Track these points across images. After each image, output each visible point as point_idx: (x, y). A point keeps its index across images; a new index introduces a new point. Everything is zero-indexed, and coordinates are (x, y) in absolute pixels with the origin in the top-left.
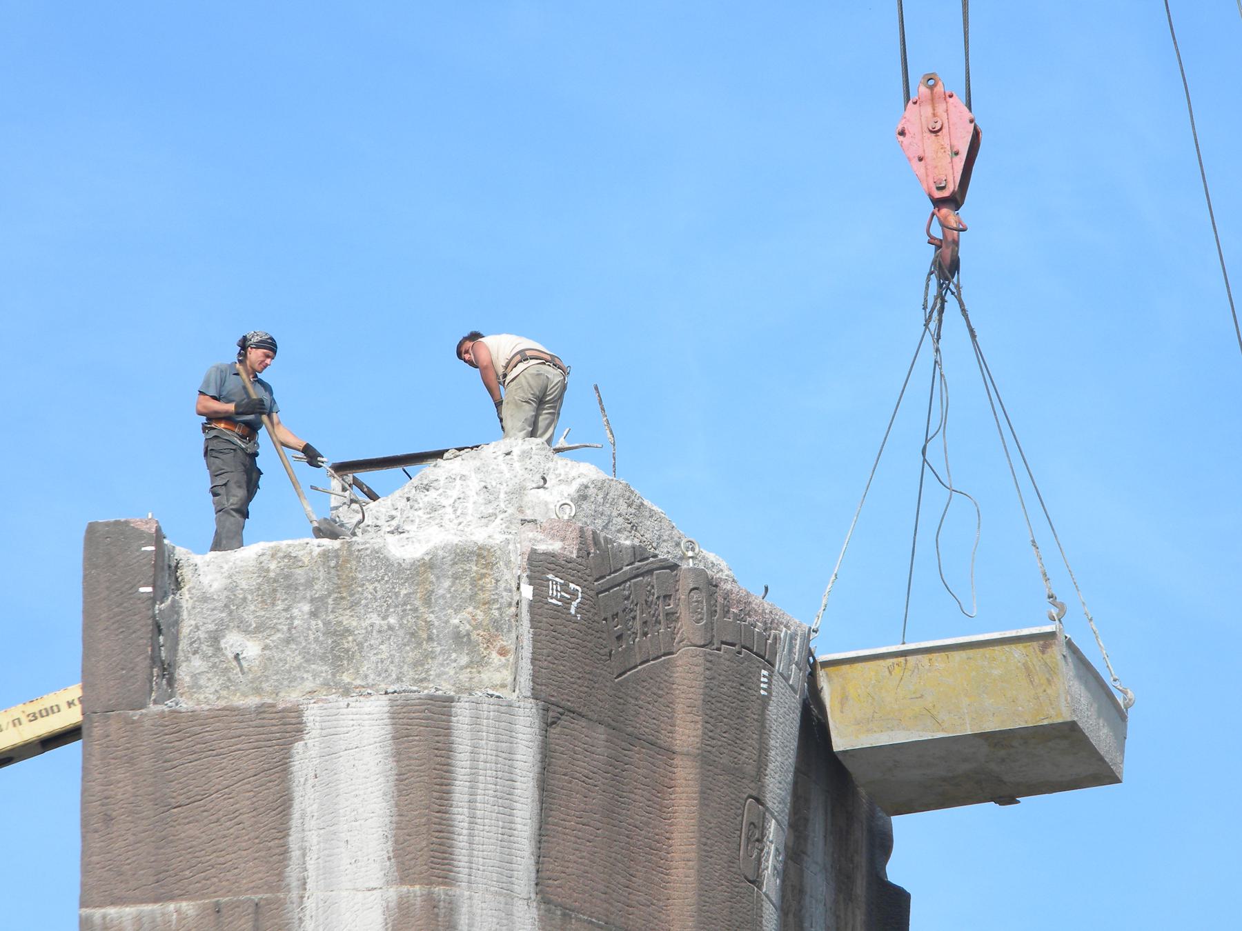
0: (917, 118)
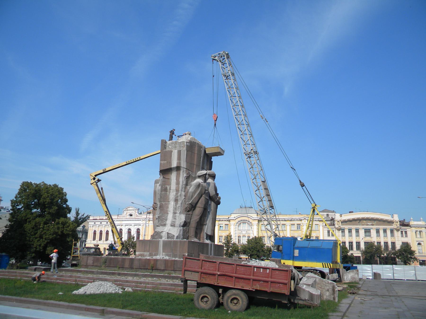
0: (214, 116)
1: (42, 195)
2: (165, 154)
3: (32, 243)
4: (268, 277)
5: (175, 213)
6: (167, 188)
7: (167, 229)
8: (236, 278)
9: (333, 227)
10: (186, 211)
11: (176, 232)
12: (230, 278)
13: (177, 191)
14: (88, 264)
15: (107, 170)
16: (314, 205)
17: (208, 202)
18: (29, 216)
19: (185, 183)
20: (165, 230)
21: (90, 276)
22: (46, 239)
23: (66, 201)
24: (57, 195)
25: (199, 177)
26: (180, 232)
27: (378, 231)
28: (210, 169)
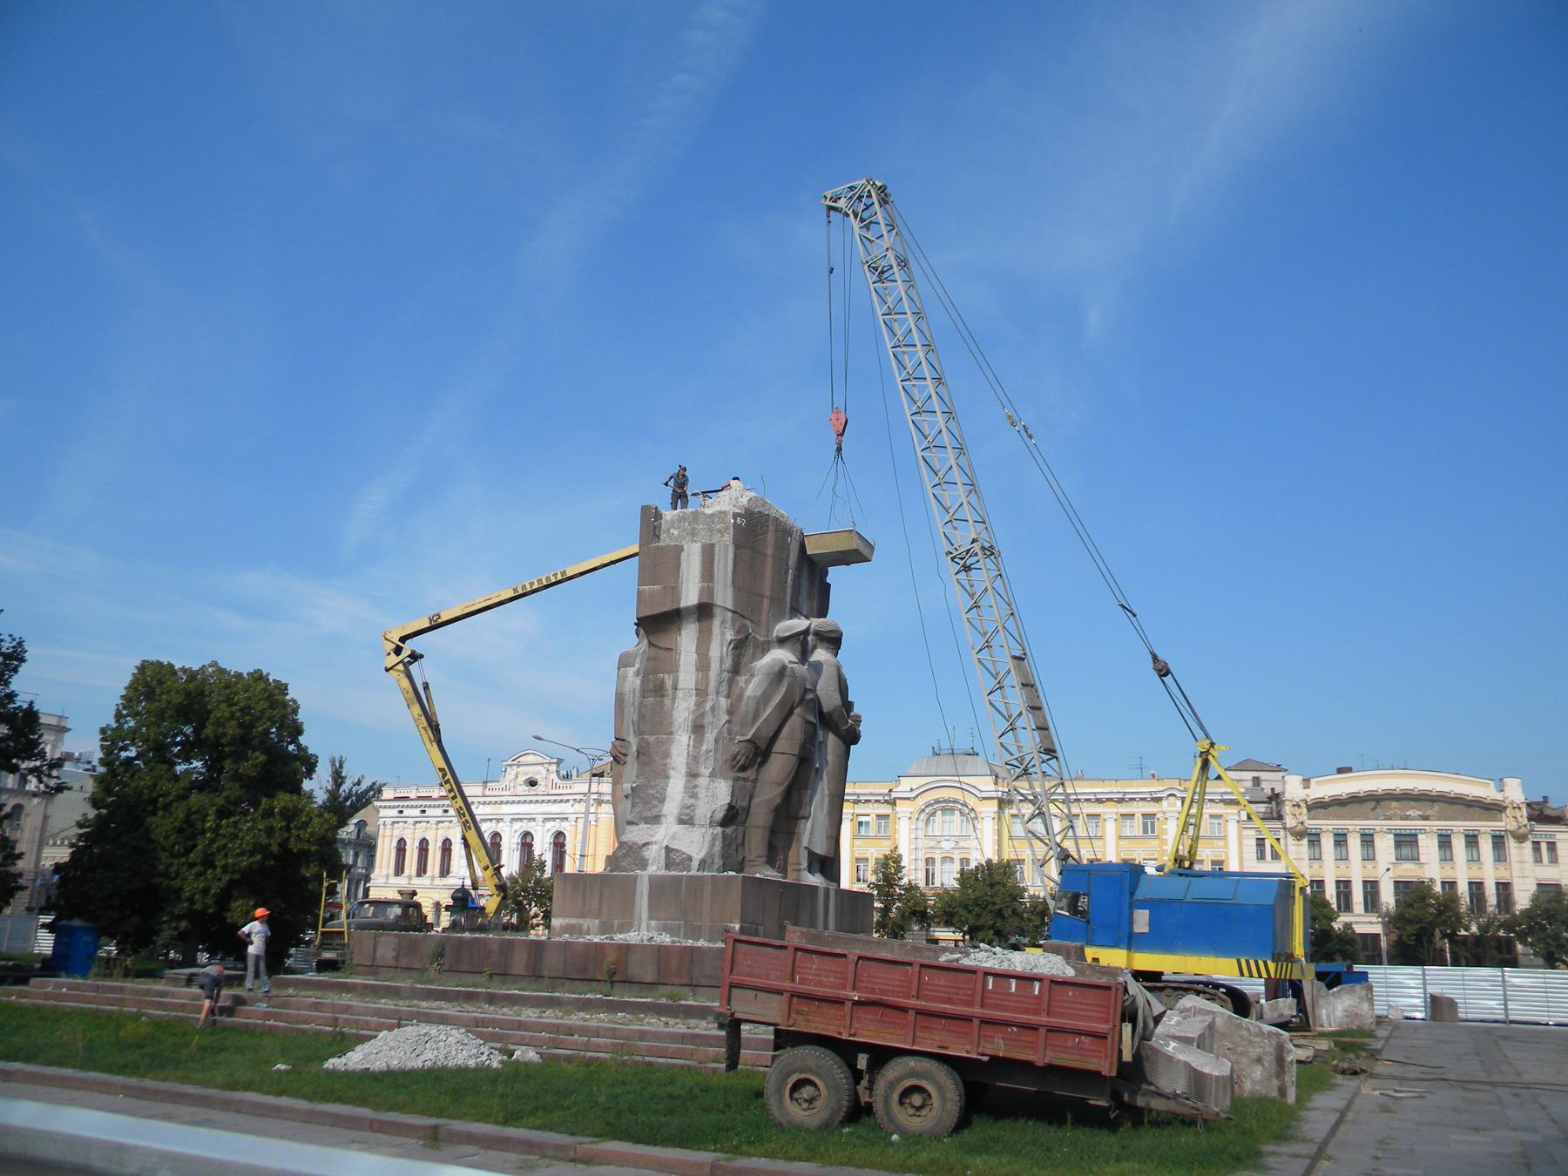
0: (834, 417)
1: (210, 712)
2: (656, 559)
3: (177, 883)
4: (1036, 1012)
5: (693, 775)
6: (662, 682)
7: (665, 834)
8: (920, 1012)
9: (1278, 824)
10: (733, 767)
11: (697, 843)
12: (900, 1013)
13: (701, 692)
14: (379, 962)
15: (444, 619)
16: (1206, 744)
17: (815, 733)
18: (165, 785)
19: (728, 664)
20: (658, 837)
21: (386, 1004)
22: (225, 869)
23: (298, 730)
24: (263, 712)
25: (782, 641)
26: (712, 845)
27: (1445, 842)
28: (823, 612)
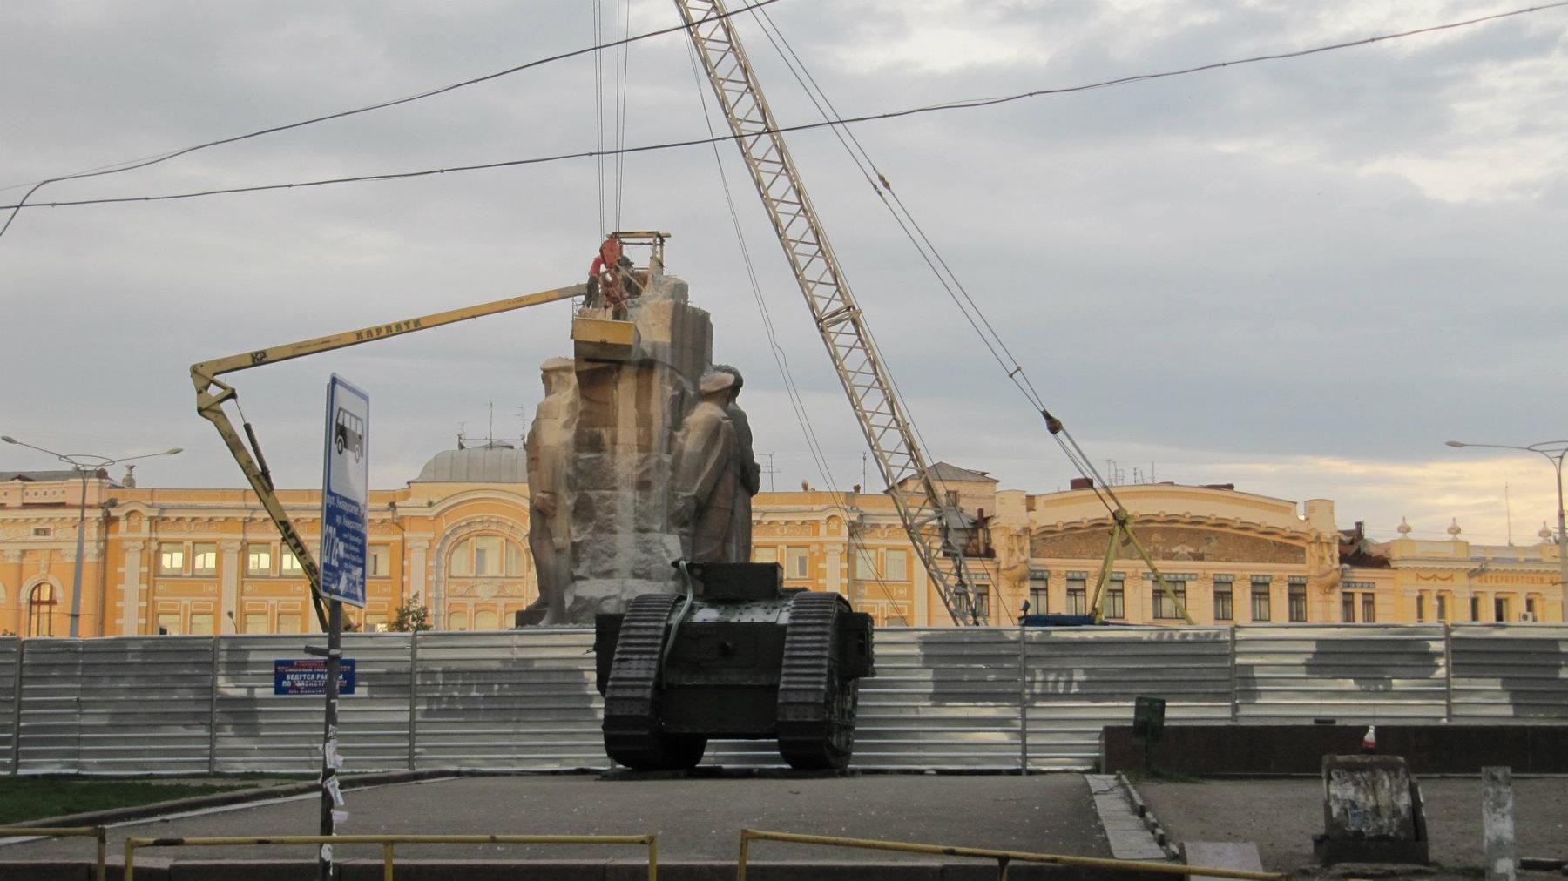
6: (599, 437)
13: (645, 447)
19: (669, 421)
